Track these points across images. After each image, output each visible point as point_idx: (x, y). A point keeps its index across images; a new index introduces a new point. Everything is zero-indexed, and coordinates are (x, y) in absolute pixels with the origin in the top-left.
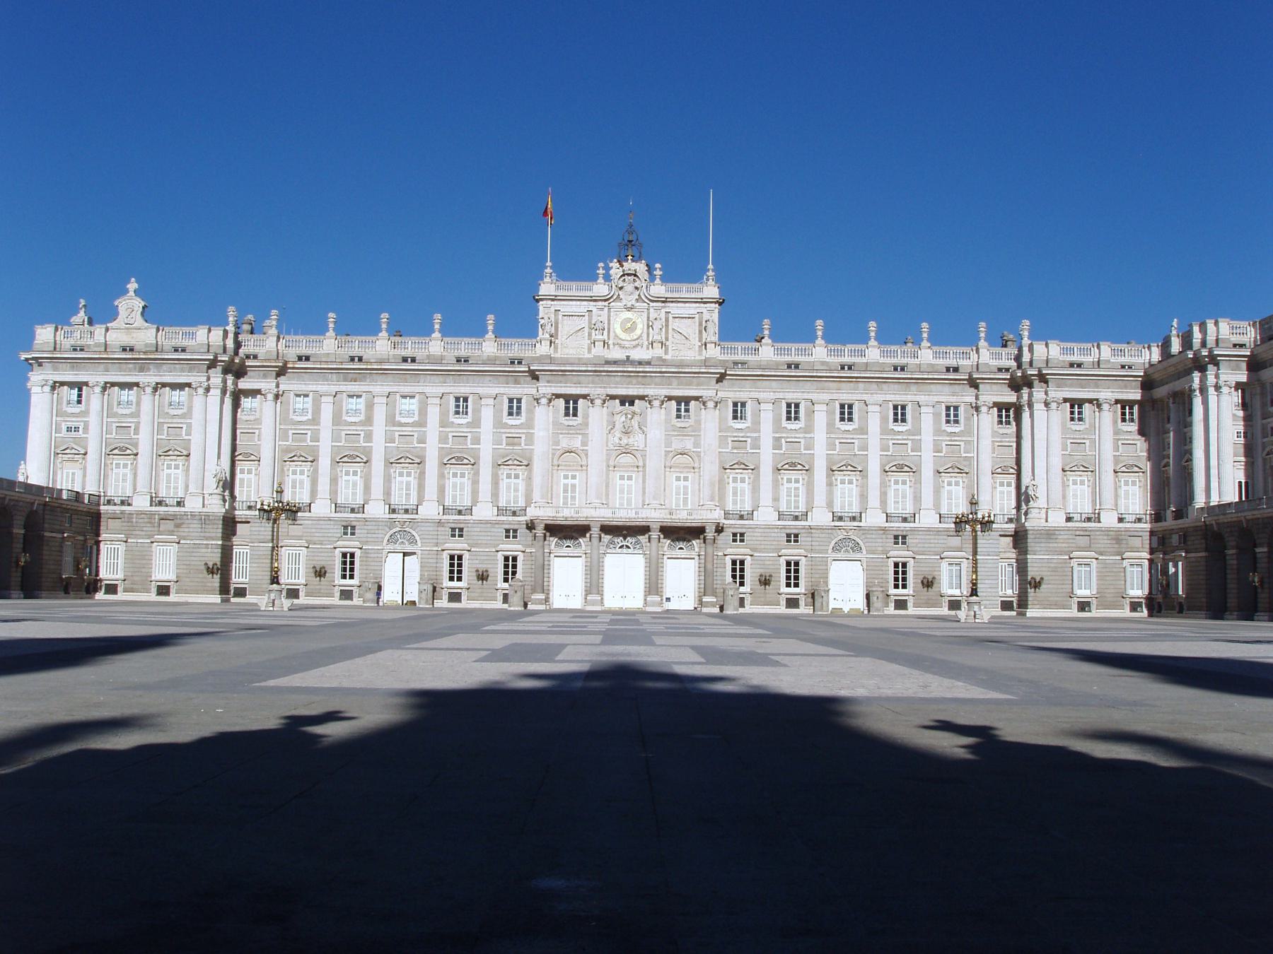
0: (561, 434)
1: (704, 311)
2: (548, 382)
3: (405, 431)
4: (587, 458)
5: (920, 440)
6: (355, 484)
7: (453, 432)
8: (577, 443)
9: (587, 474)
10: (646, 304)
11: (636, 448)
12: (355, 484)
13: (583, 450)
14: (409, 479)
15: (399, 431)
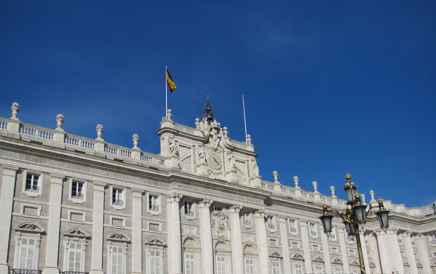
0: (185, 224)
1: (250, 160)
2: (179, 186)
3: (76, 210)
4: (200, 244)
5: (341, 246)
6: (31, 252)
7: (113, 215)
8: (194, 232)
9: (201, 255)
10: (222, 149)
11: (226, 239)
12: (31, 252)
13: (198, 238)
14: (79, 250)
15: (71, 209)
